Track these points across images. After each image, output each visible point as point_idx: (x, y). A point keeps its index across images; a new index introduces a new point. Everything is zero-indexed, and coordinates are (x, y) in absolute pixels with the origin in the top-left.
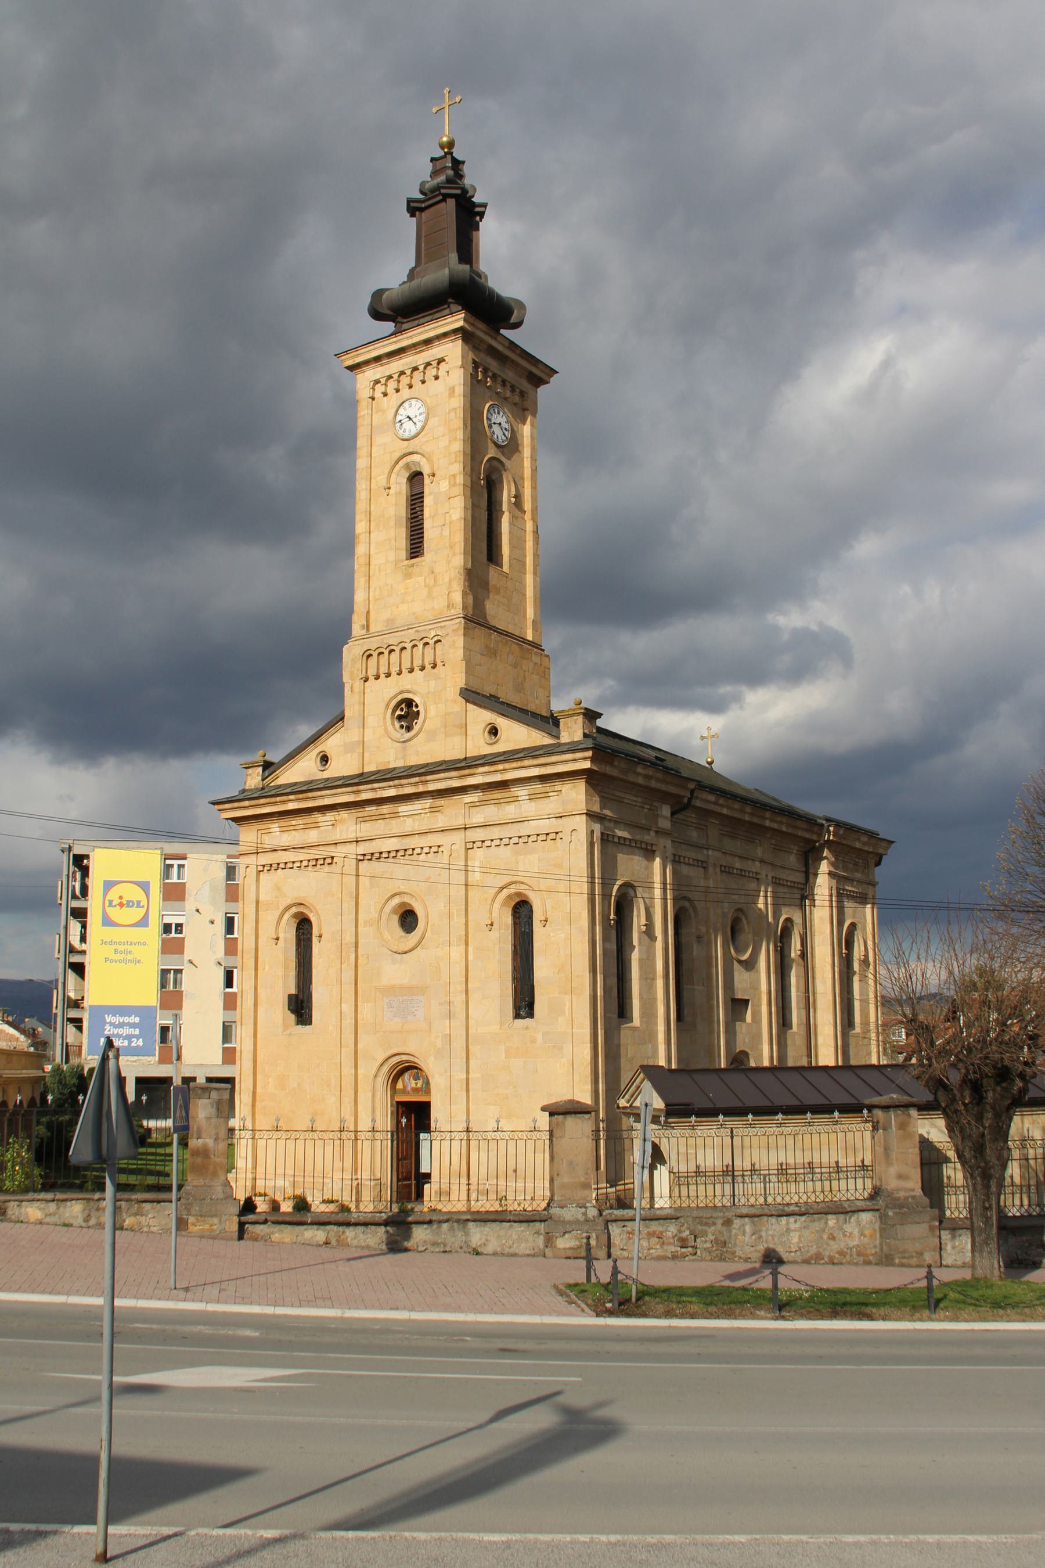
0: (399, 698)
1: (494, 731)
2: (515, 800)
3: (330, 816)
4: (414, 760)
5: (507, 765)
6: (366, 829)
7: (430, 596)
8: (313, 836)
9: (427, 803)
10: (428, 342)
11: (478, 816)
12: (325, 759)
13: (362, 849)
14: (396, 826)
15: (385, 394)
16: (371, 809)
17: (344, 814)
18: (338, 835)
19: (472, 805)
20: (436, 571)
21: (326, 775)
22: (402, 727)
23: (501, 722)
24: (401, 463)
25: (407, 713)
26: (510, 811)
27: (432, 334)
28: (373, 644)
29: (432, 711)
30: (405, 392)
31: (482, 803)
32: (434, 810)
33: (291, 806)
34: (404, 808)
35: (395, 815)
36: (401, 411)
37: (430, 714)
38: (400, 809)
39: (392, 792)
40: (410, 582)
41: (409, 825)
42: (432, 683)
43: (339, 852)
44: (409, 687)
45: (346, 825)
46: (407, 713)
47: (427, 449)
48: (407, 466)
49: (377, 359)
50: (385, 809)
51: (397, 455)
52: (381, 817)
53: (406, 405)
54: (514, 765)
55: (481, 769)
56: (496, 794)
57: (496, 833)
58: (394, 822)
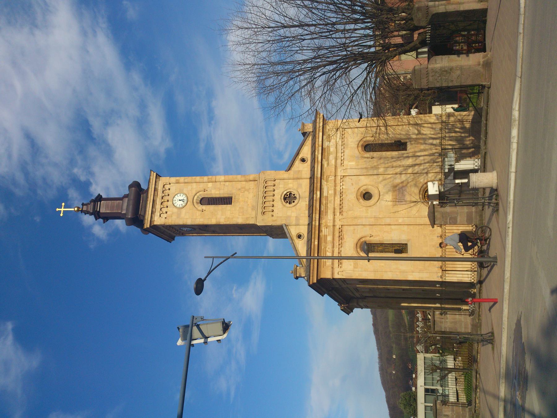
0: (283, 200)
1: (303, 160)
2: (328, 147)
3: (323, 229)
4: (307, 194)
5: (317, 143)
6: (330, 212)
7: (248, 190)
8: (329, 238)
9: (324, 183)
10: (155, 190)
11: (333, 162)
12: (299, 236)
13: (338, 214)
14: (331, 198)
15: (166, 212)
16: (323, 208)
17: (323, 222)
18: (330, 224)
19: (328, 164)
20: (240, 187)
21: (306, 238)
22: (294, 195)
23: (300, 156)
24: (195, 204)
25: (289, 198)
26: (332, 149)
27: (153, 186)
28: (260, 211)
29: (291, 186)
30: (170, 203)
31: (328, 160)
32: (327, 181)
33: (316, 243)
34: (325, 194)
35: (327, 198)
36: (176, 205)
37: (292, 186)
38: (325, 195)
39: (318, 193)
40: (241, 199)
41: (331, 192)
42: (281, 186)
43: (338, 224)
44: (280, 196)
45: (328, 219)
46: (289, 198)
47: (194, 193)
48: (197, 203)
49: (152, 213)
50: (324, 201)
51: (192, 206)
52: (327, 204)
53: (174, 202)
54: (317, 140)
55: (316, 153)
56: (326, 154)
57: (339, 155)
58: (329, 199)
